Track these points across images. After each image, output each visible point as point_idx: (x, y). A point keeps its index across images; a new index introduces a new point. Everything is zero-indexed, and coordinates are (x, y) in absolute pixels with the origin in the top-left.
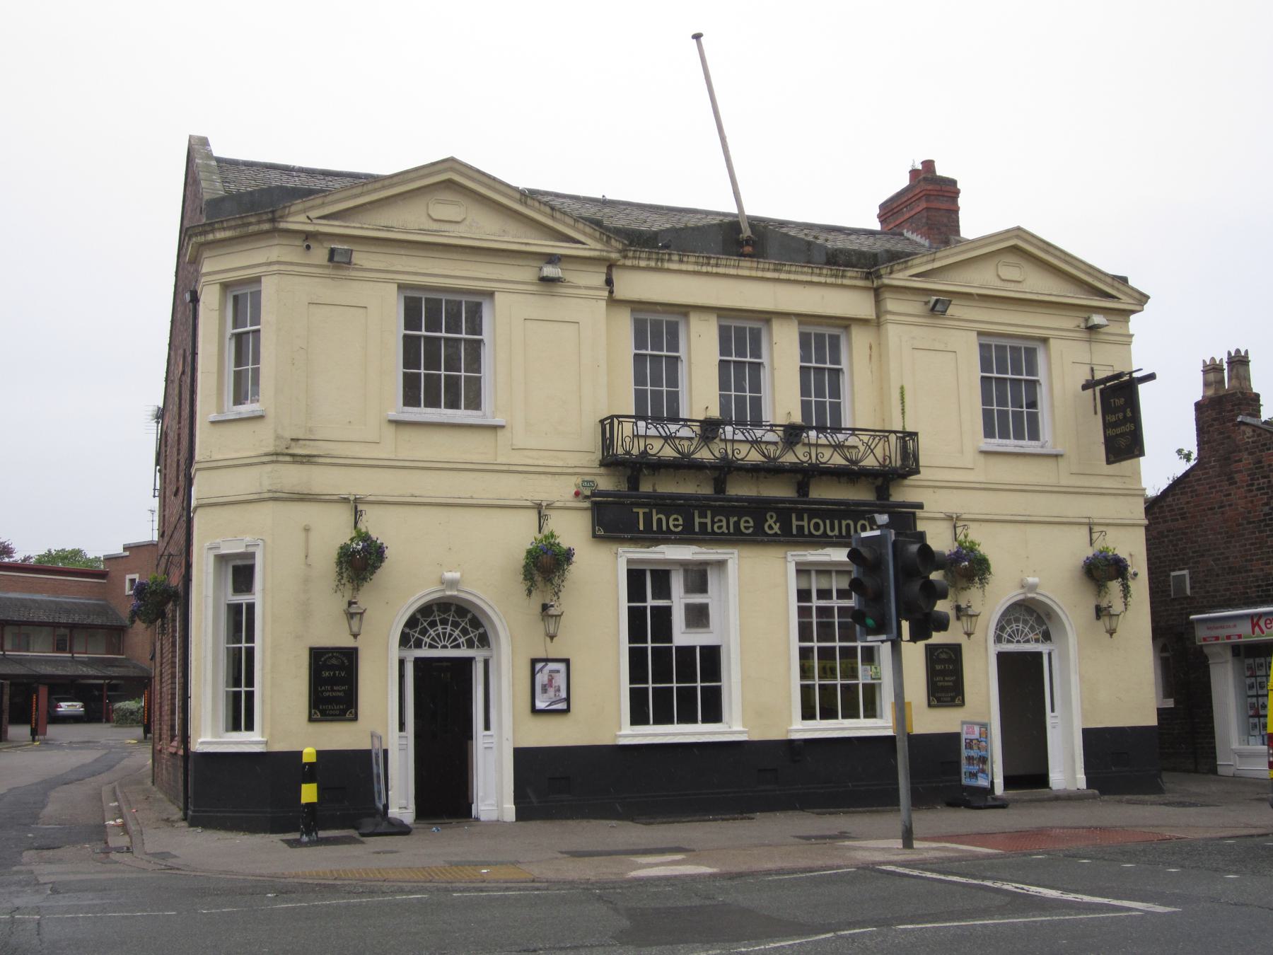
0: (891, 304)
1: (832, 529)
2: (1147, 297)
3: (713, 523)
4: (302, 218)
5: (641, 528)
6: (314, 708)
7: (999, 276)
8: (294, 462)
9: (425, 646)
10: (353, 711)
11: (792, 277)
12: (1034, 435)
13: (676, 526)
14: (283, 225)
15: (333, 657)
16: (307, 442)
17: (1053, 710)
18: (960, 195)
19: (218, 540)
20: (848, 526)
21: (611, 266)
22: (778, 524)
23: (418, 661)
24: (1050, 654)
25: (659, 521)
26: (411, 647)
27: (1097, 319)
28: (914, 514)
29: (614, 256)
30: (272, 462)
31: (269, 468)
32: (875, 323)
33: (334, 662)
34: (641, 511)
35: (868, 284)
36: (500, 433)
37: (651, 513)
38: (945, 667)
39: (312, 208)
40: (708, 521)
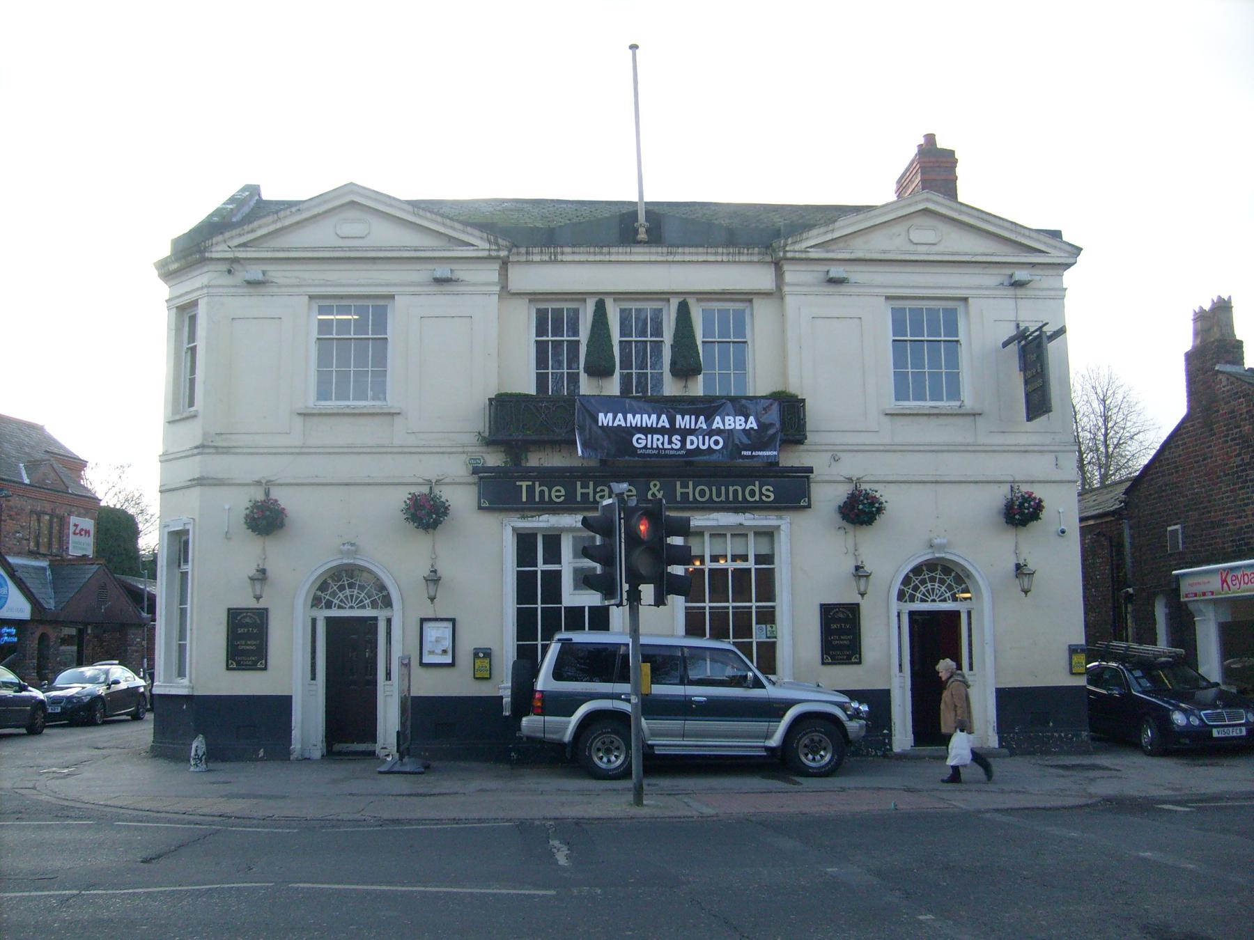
0: (792, 275)
1: (719, 495)
2: (1079, 250)
3: (595, 493)
4: (224, 247)
5: (524, 499)
6: (231, 659)
7: (911, 241)
8: (217, 453)
9: (335, 607)
10: (264, 661)
11: (687, 258)
12: (955, 394)
13: (558, 497)
14: (207, 255)
15: (246, 617)
16: (228, 436)
17: (971, 669)
18: (958, 164)
19: (168, 520)
20: (736, 492)
21: (505, 263)
22: (662, 492)
23: (329, 620)
24: (969, 613)
25: (542, 492)
26: (322, 608)
27: (1021, 275)
28: (808, 477)
29: (503, 254)
30: (199, 454)
31: (198, 457)
32: (777, 294)
33: (248, 620)
34: (524, 484)
35: (768, 259)
36: (397, 419)
37: (534, 484)
38: (841, 626)
39: (232, 238)
40: (591, 491)
